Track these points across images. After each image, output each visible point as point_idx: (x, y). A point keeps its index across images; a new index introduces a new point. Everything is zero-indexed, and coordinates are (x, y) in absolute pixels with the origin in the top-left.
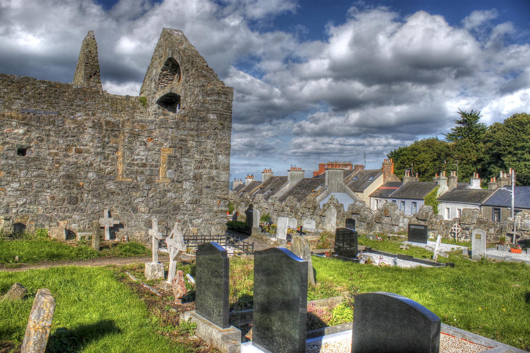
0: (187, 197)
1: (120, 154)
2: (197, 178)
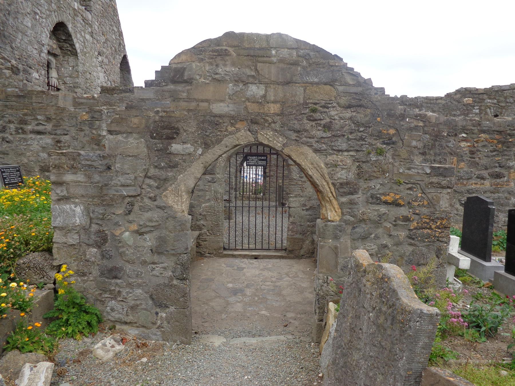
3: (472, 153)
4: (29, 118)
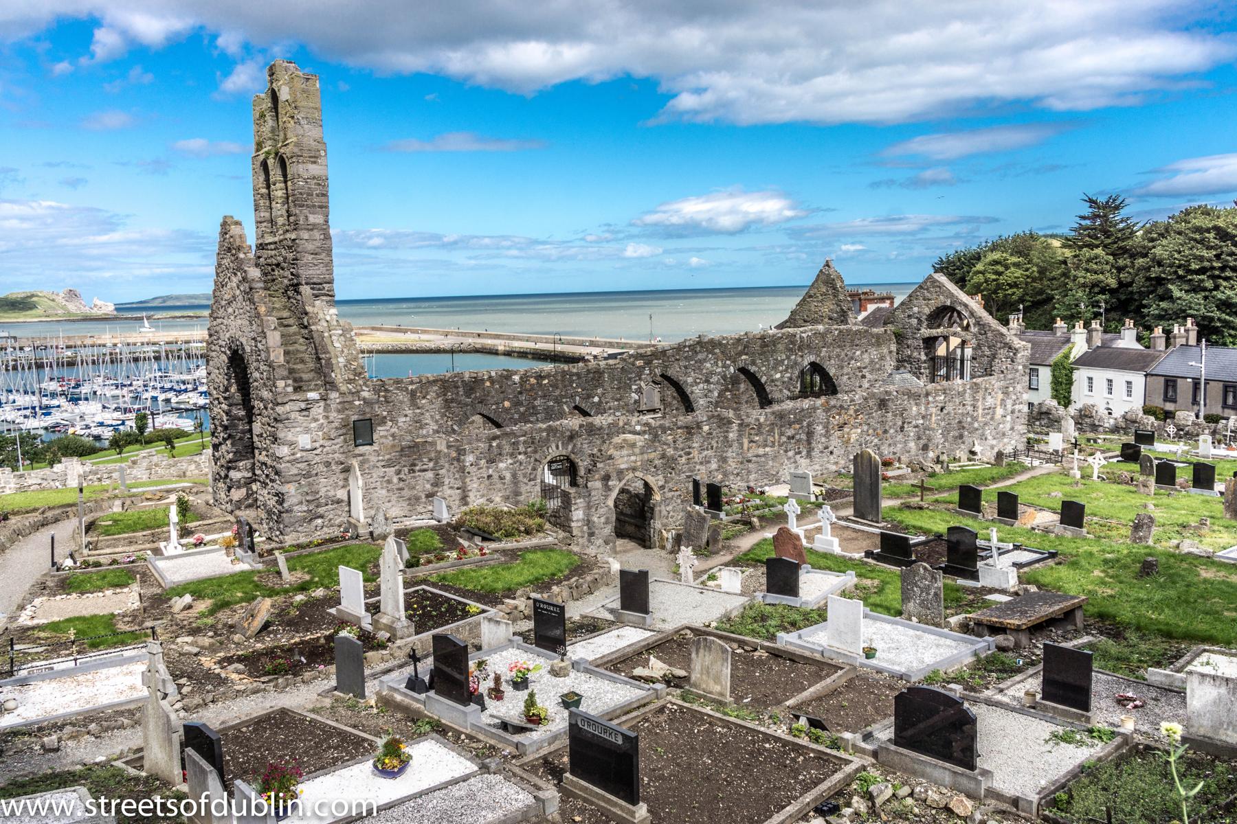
0: (1008, 426)
1: (980, 403)
2: (1013, 412)
3: (674, 442)
4: (417, 462)
